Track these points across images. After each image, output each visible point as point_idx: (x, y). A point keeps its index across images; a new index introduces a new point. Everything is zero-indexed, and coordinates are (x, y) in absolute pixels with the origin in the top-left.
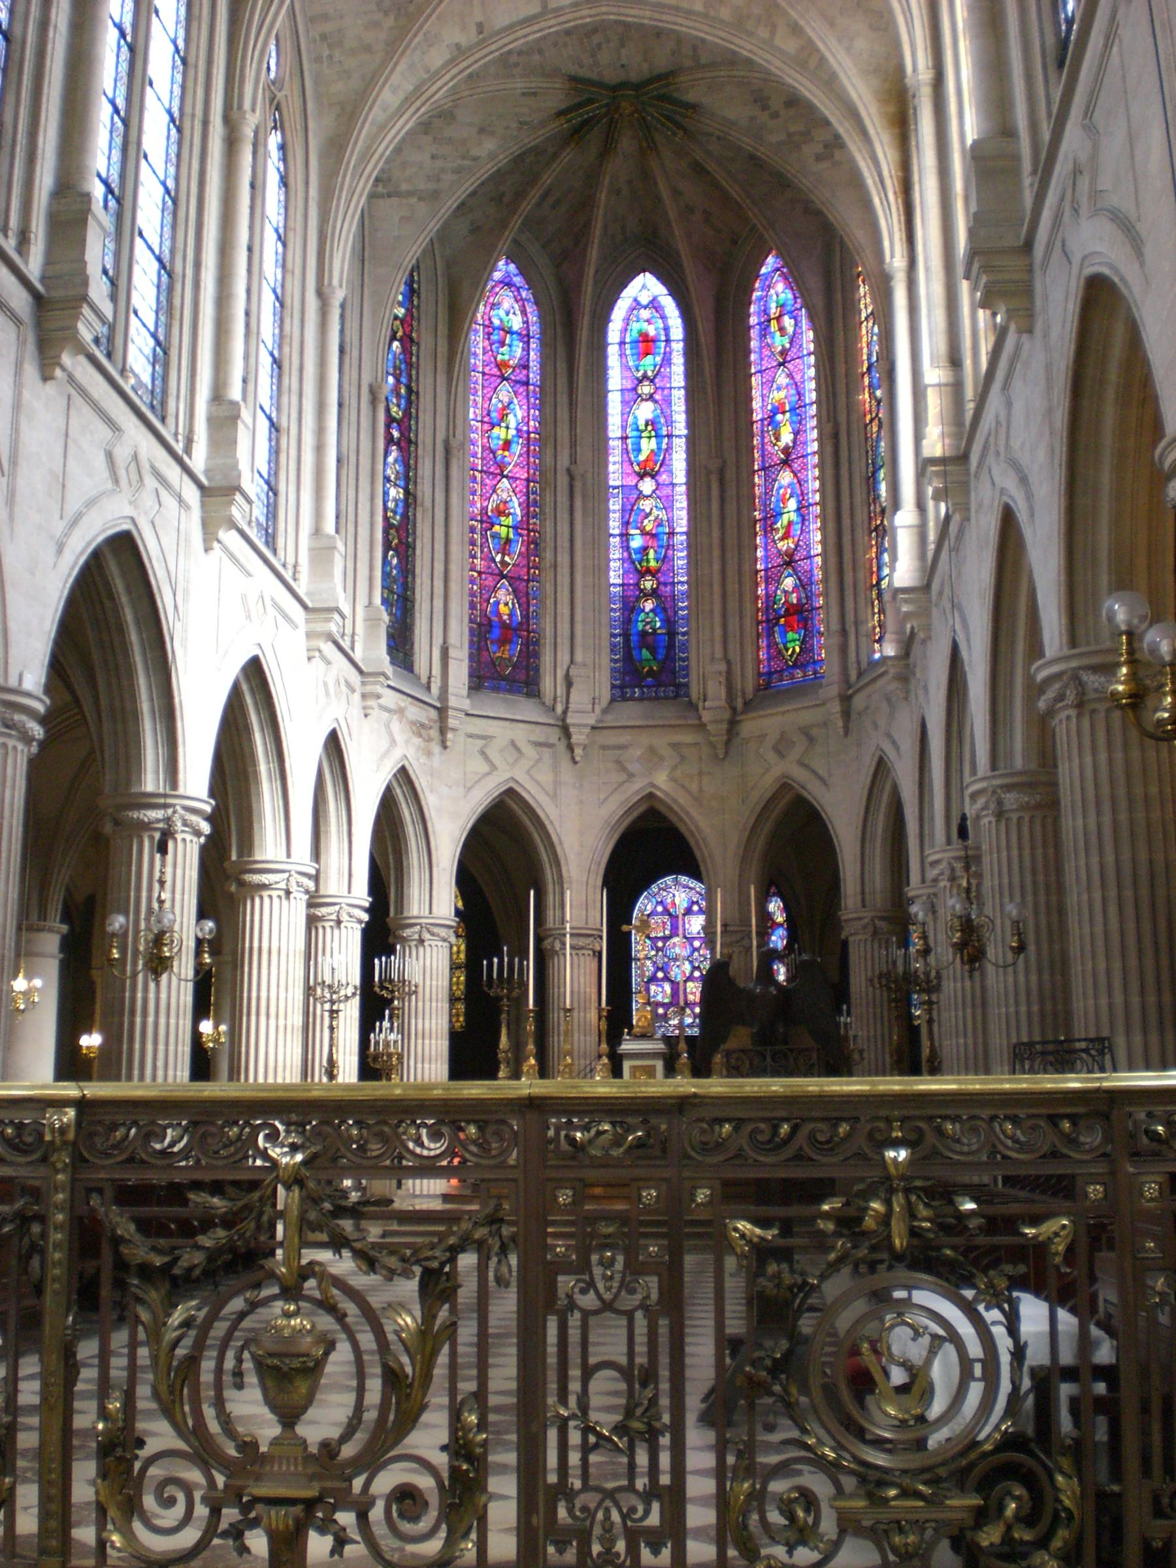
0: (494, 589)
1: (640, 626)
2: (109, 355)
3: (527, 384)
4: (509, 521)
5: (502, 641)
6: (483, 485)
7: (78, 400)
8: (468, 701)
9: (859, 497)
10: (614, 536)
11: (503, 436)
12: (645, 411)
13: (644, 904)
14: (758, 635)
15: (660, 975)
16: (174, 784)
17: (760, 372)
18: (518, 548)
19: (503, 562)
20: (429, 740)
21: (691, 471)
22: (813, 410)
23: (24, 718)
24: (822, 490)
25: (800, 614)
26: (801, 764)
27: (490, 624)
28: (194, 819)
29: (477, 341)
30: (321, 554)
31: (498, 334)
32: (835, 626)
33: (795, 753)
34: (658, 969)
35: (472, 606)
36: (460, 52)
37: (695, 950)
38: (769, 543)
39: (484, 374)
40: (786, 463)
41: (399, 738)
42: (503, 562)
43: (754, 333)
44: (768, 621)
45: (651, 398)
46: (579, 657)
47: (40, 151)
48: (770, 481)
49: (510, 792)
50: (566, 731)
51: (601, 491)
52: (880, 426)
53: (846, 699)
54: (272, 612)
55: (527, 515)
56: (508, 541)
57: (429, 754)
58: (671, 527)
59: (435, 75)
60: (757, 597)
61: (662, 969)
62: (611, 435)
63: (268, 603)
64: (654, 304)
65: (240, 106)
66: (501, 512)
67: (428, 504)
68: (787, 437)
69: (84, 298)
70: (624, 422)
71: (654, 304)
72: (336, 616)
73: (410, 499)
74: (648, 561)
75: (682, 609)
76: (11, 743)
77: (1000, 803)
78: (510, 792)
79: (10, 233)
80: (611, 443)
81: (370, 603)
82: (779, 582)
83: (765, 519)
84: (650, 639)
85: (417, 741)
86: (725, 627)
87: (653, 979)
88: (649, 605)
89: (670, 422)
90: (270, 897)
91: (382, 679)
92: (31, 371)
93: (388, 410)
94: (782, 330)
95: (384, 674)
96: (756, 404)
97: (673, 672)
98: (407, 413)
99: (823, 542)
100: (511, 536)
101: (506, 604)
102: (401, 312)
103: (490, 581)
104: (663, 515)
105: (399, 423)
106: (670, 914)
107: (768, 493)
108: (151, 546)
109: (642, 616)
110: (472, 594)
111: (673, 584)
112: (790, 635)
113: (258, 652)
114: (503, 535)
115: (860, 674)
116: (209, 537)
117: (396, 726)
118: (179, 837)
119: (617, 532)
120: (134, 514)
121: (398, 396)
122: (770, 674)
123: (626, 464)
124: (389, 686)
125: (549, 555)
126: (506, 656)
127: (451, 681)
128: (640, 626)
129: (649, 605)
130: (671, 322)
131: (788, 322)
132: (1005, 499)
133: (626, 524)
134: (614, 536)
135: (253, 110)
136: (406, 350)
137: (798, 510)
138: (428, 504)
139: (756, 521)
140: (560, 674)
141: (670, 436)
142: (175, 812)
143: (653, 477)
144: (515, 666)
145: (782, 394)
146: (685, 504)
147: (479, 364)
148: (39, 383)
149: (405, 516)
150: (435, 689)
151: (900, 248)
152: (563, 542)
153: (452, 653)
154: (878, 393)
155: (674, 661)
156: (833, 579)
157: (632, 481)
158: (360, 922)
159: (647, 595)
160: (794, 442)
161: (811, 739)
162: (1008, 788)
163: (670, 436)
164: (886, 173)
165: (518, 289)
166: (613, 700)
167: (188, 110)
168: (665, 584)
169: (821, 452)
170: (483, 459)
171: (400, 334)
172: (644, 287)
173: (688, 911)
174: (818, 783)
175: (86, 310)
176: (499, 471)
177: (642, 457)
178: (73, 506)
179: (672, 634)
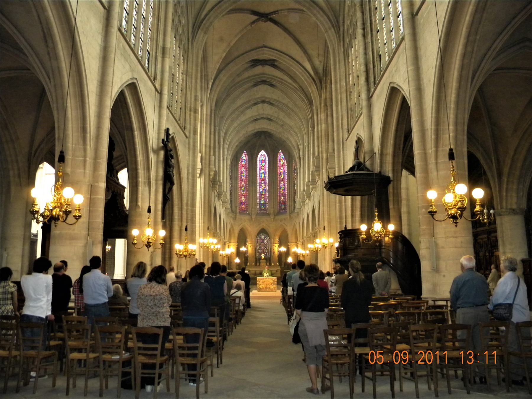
0: (242, 197)
5: (242, 205)
12: (262, 171)
24: (287, 185)
25: (284, 202)
29: (240, 161)
36: (244, 134)
38: (280, 192)
40: (282, 180)
43: (278, 161)
48: (280, 183)
57: (234, 222)
59: (241, 138)
66: (242, 186)
68: (283, 177)
71: (264, 155)
88: (263, 199)
89: (266, 173)
96: (278, 171)
107: (280, 184)
122: (279, 210)
129: (263, 199)
131: (283, 160)
133: (260, 187)
169: (287, 180)
173: (264, 239)
176: (242, 180)
179: (266, 204)
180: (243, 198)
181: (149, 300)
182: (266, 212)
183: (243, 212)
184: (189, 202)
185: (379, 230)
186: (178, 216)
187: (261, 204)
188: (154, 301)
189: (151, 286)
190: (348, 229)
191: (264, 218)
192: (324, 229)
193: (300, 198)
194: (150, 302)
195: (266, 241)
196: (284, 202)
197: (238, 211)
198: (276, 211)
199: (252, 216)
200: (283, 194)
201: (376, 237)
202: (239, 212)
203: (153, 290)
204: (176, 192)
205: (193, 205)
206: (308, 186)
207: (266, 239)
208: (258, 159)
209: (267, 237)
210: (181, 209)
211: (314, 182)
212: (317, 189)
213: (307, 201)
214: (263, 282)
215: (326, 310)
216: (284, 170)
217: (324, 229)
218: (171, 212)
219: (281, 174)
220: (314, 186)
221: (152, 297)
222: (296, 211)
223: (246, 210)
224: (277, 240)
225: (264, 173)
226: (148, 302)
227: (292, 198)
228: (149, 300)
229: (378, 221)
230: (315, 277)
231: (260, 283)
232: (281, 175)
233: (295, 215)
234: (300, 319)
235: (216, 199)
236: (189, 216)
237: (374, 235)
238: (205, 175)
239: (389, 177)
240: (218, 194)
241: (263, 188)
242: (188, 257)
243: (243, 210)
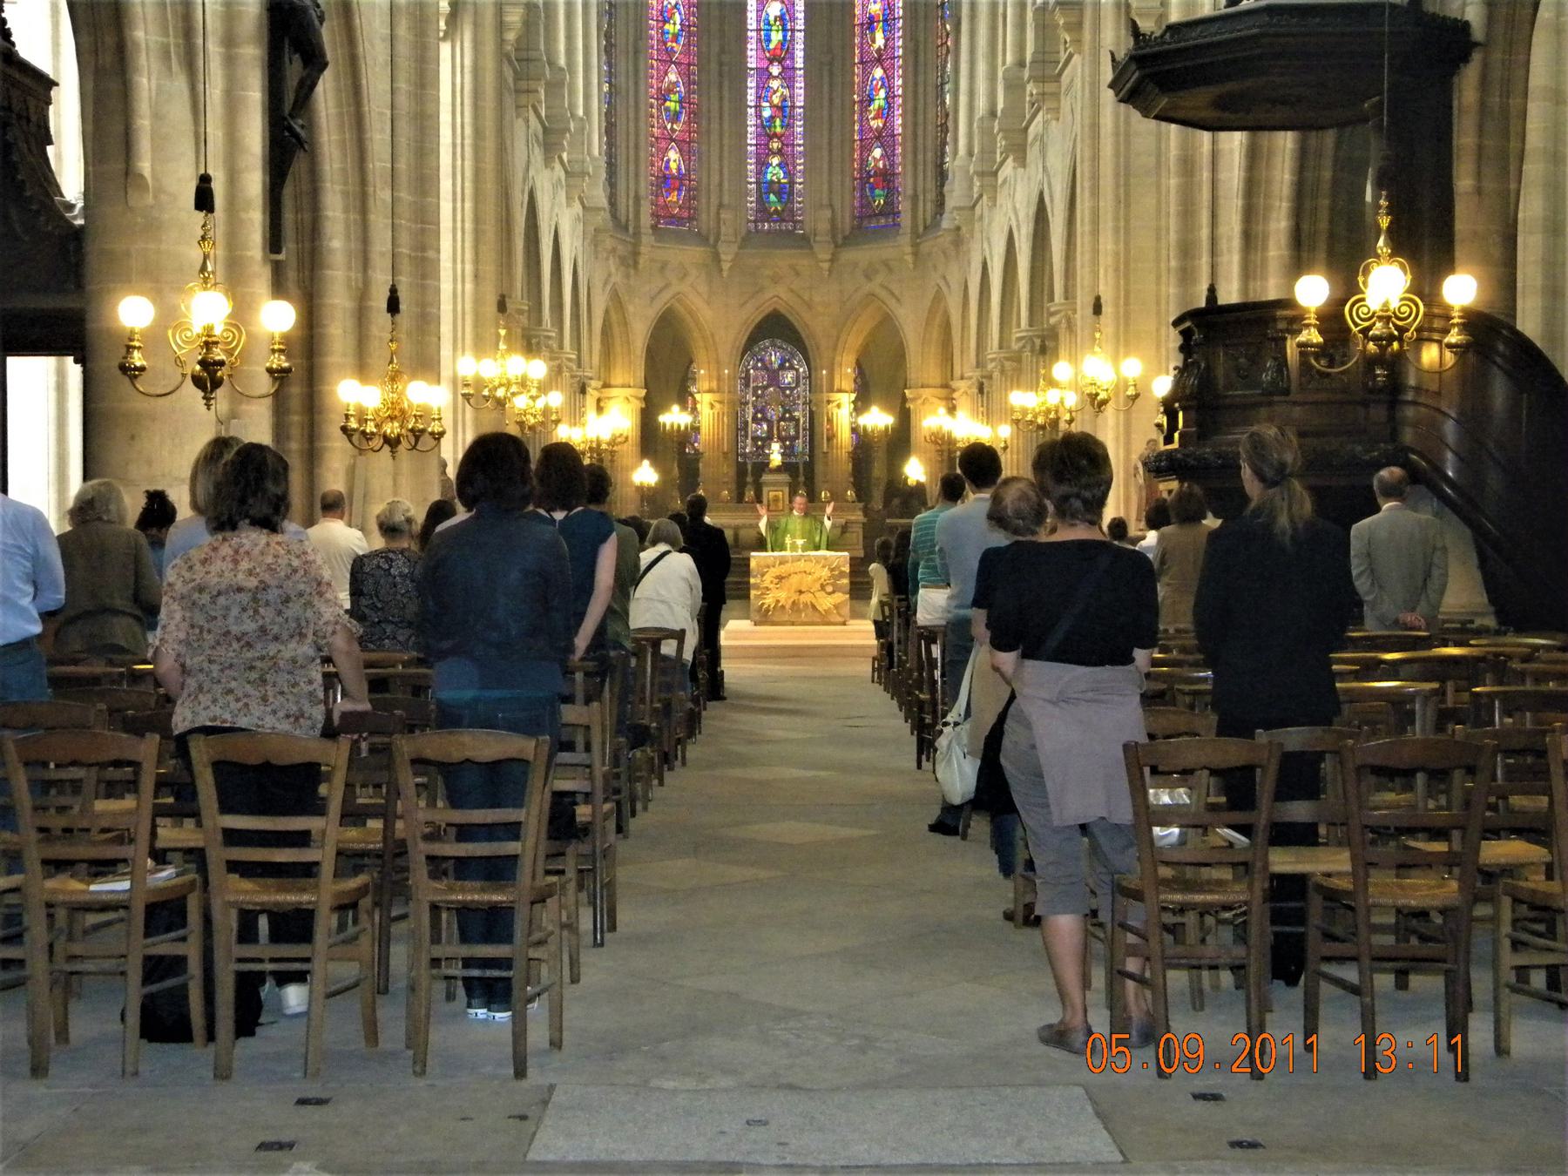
0: (667, 150)
1: (769, 176)
4: (674, 97)
9: (930, 99)
14: (854, 189)
18: (683, 117)
19: (672, 129)
20: (628, 266)
21: (806, 58)
22: (900, 24)
24: (904, 86)
25: (886, 178)
26: (883, 286)
32: (910, 192)
33: (879, 279)
38: (863, 120)
40: (879, 61)
41: (613, 270)
42: (672, 129)
44: (861, 178)
46: (726, 200)
48: (866, 74)
51: (739, 72)
53: (915, 245)
55: (689, 92)
57: (628, 276)
62: (749, 27)
66: (670, 91)
67: (624, 93)
68: (880, 40)
77: (1003, 366)
78: (679, 301)
80: (749, 34)
82: (870, 151)
83: (861, 102)
85: (622, 268)
86: (830, 182)
88: (775, 161)
89: (793, 19)
99: (904, 125)
103: (663, 145)
104: (786, 92)
107: (864, 83)
109: (770, 169)
111: (793, 145)
115: (926, 228)
117: (611, 261)
119: (753, 104)
122: (861, 218)
123: (760, 52)
125: (704, 123)
128: (769, 176)
129: (775, 161)
133: (759, 98)
137: (886, 98)
138: (624, 93)
143: (780, 63)
146: (802, 85)
152: (715, 114)
155: (793, 203)
156: (910, 156)
157: (765, 64)
159: (774, 154)
160: (885, 46)
161: (890, 270)
162: (1007, 359)
163: (793, 31)
168: (787, 145)
169: (904, 57)
174: (894, 301)
176: (667, 58)
177: (772, 46)
179: (792, 183)
180: (673, 155)
181: (235, 611)
182: (790, 226)
183: (672, 225)
184: (402, 165)
185: (1394, 304)
186: (348, 238)
187: (765, 187)
188: (256, 612)
189: (237, 552)
190: (1221, 301)
191: (783, 259)
192: (1097, 309)
193: (970, 153)
194: (238, 620)
195: (788, 377)
196: (886, 178)
197: (646, 220)
198: (846, 223)
199: (722, 248)
200: (879, 131)
201: (1376, 339)
202: (654, 227)
203: (245, 565)
204: (332, 111)
205: (425, 182)
206: (1014, 86)
207: (792, 368)
209: (793, 356)
210: (361, 202)
211: (1047, 68)
212: (1065, 104)
213: (1008, 170)
214: (780, 578)
215: (1140, 655)
217: (1097, 309)
218: (307, 216)
219: (871, 22)
220: (1050, 87)
221: (244, 598)
222: (946, 224)
223: (690, 219)
224: (846, 374)
225: (781, 18)
226: (231, 620)
227: (930, 155)
228: (235, 611)
229: (1391, 256)
230: (1087, 494)
231: (768, 578)
232: (872, 30)
233: (945, 240)
234: (1013, 697)
235: (538, 154)
236: (405, 238)
237: (1365, 331)
238: (476, 25)
239: (1466, 25)
240: (545, 129)
241: (776, 100)
242: (404, 444)
243: (674, 219)
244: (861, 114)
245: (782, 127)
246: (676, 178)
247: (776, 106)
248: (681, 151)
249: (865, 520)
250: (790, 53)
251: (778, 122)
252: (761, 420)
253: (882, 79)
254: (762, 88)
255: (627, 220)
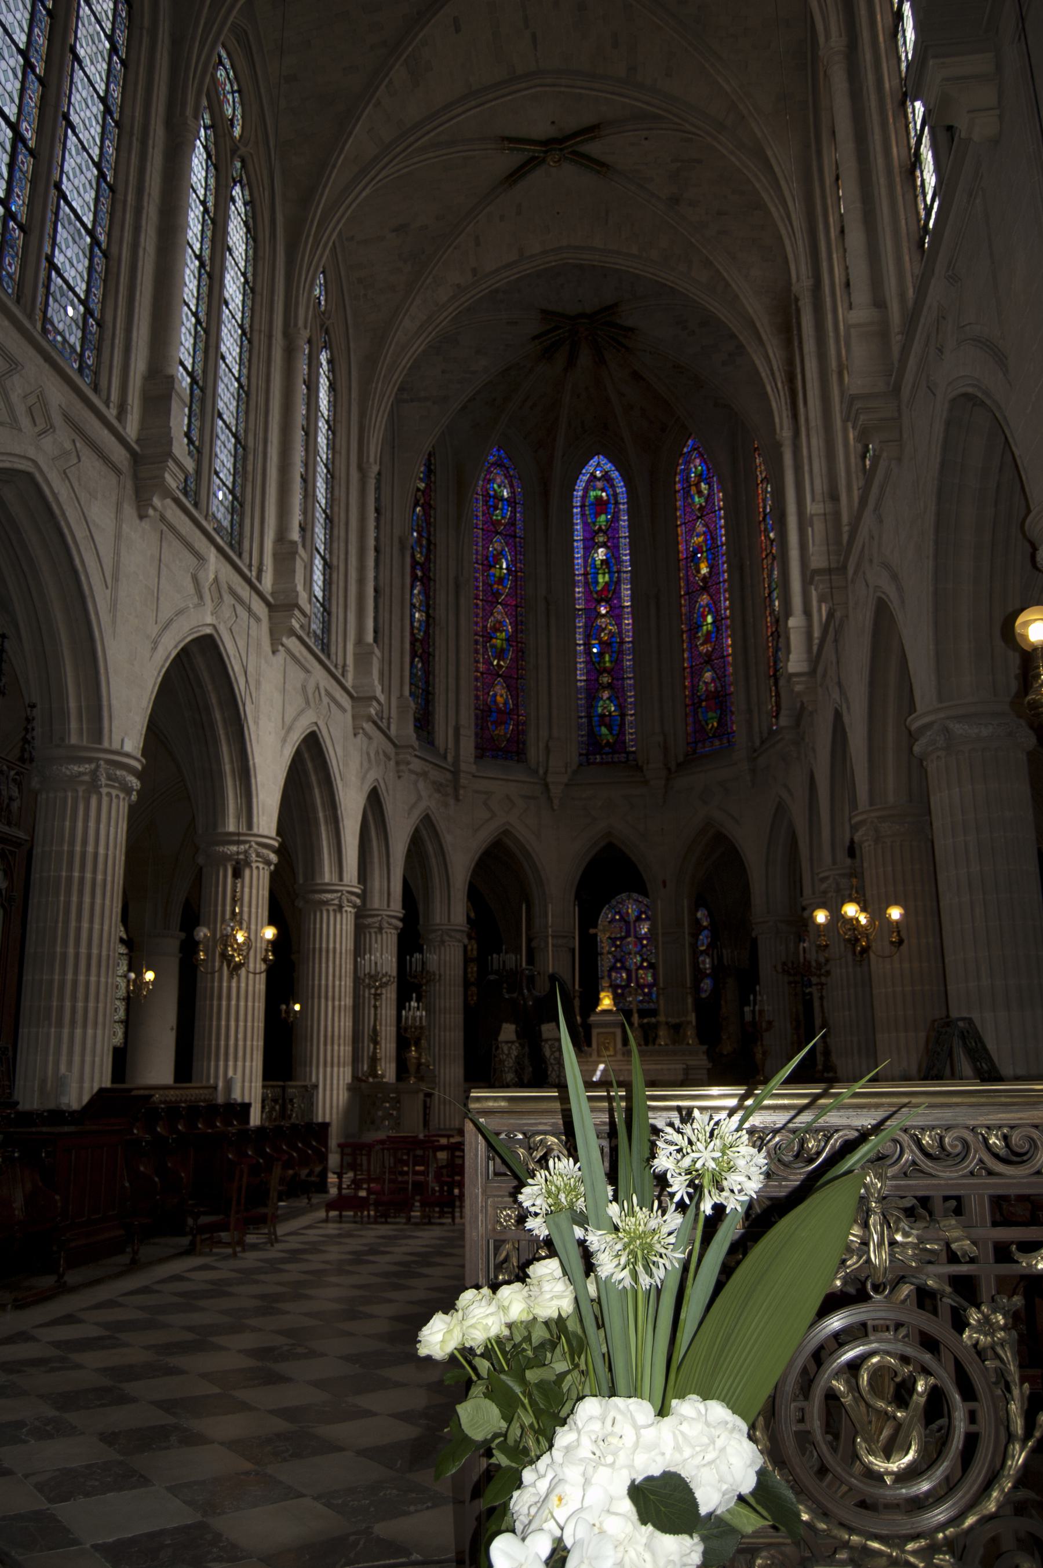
0: (492, 685)
1: (600, 710)
2: (196, 505)
3: (515, 536)
5: (497, 724)
6: (484, 610)
7: (170, 536)
8: (474, 767)
10: (580, 645)
11: (497, 574)
12: (601, 554)
13: (606, 915)
14: (686, 715)
15: (619, 965)
16: (250, 825)
17: (685, 523)
23: (124, 773)
27: (490, 710)
28: (265, 851)
30: (362, 659)
31: (492, 501)
34: (617, 961)
35: (477, 697)
37: (643, 946)
38: (693, 647)
39: (483, 529)
40: (705, 589)
43: (678, 496)
44: (693, 704)
45: (604, 545)
47: (134, 343)
48: (693, 602)
49: (506, 832)
50: (546, 786)
52: (774, 558)
54: (326, 700)
55: (516, 631)
56: (502, 650)
58: (622, 638)
60: (685, 687)
61: (620, 961)
63: (323, 692)
64: (606, 477)
65: (296, 325)
68: (704, 570)
69: (170, 454)
70: (586, 562)
71: (606, 477)
72: (375, 703)
73: (429, 620)
74: (605, 662)
75: (630, 697)
76: (114, 792)
79: (111, 405)
81: (402, 695)
82: (701, 675)
84: (607, 719)
85: (437, 795)
87: (613, 968)
88: (606, 694)
89: (619, 561)
90: (328, 911)
91: (411, 750)
92: (129, 510)
93: (413, 556)
94: (700, 493)
95: (412, 747)
97: (624, 742)
98: (428, 559)
100: (505, 646)
101: (501, 696)
102: (422, 486)
104: (613, 629)
105: (422, 565)
106: (625, 921)
108: (229, 647)
109: (601, 703)
110: (477, 689)
111: (623, 679)
112: (710, 714)
113: (315, 728)
114: (499, 646)
115: (762, 742)
116: (276, 644)
117: (421, 785)
118: (254, 865)
120: (215, 622)
121: (421, 546)
124: (416, 756)
126: (502, 733)
127: (462, 752)
129: (606, 694)
130: (618, 490)
132: (879, 594)
133: (588, 637)
134: (580, 645)
135: (306, 328)
136: (426, 513)
139: (683, 632)
140: (542, 745)
141: (619, 572)
142: (250, 847)
143: (607, 602)
144: (508, 741)
145: (701, 539)
147: (480, 523)
148: (138, 521)
149: (427, 633)
150: (450, 758)
151: (787, 423)
153: (462, 731)
154: (772, 535)
155: (624, 735)
158: (396, 928)
159: (605, 688)
160: (710, 573)
164: (775, 368)
165: (507, 469)
166: (581, 765)
167: (256, 327)
168: (618, 680)
170: (483, 591)
171: (422, 501)
172: (598, 465)
173: (638, 919)
175: (171, 464)
177: (599, 588)
178: (165, 614)
179: (623, 715)
182: (623, 757)
196: (720, 699)
200: (709, 655)
208: (577, 502)
216: (711, 535)
240: (136, 458)
244: (690, 643)
245: (611, 661)
246: (499, 711)
247: (605, 643)
248: (508, 687)
249: (710, 1066)
250: (617, 593)
251: (607, 658)
252: (620, 968)
253: (708, 605)
254: (591, 631)
255: (446, 750)
